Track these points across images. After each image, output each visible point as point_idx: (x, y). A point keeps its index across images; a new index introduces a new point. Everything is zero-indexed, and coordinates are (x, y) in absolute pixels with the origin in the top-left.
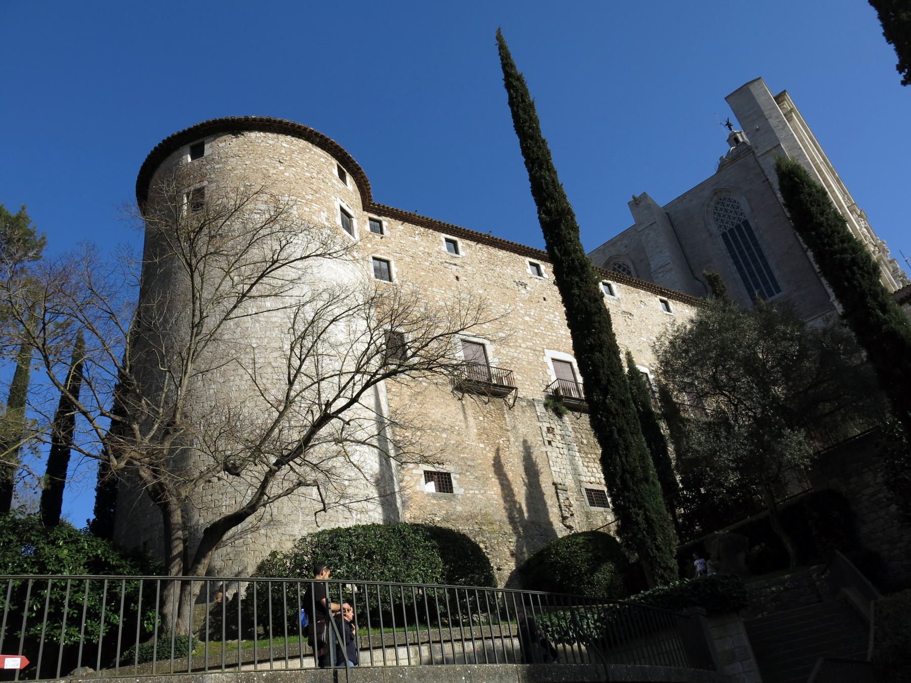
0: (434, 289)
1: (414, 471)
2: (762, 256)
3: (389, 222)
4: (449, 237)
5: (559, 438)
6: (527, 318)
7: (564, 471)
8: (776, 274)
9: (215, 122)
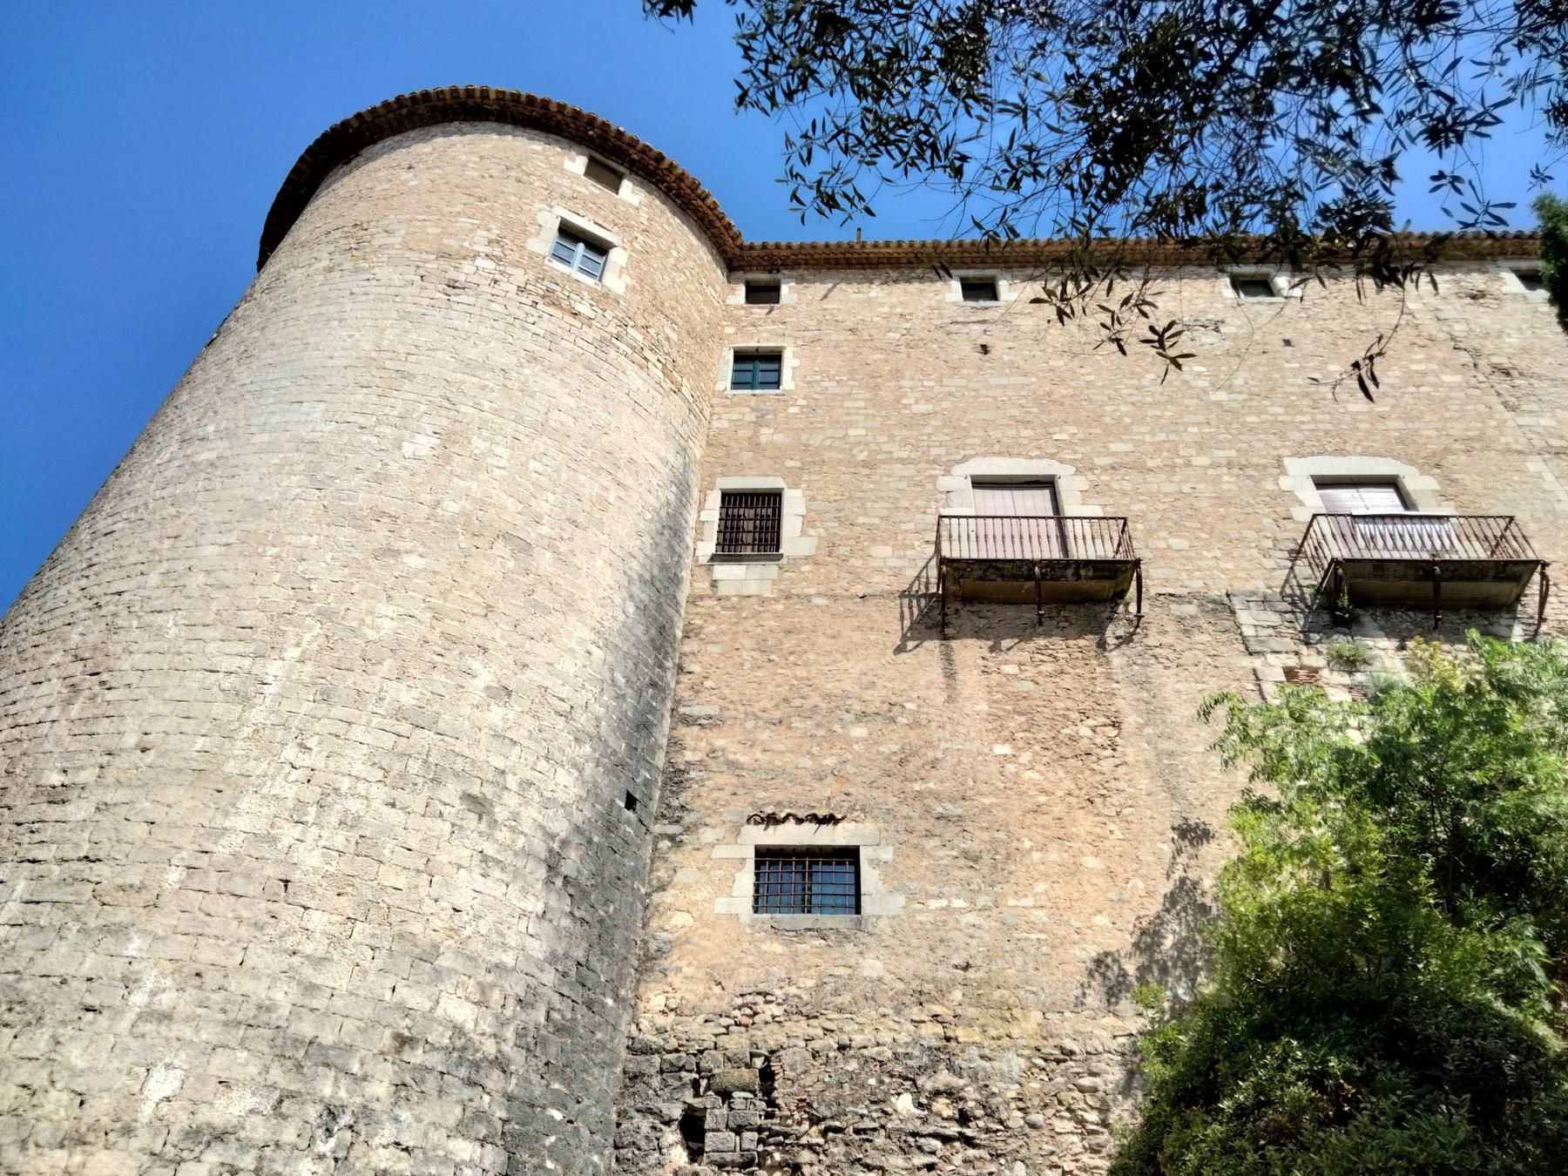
1: (720, 852)
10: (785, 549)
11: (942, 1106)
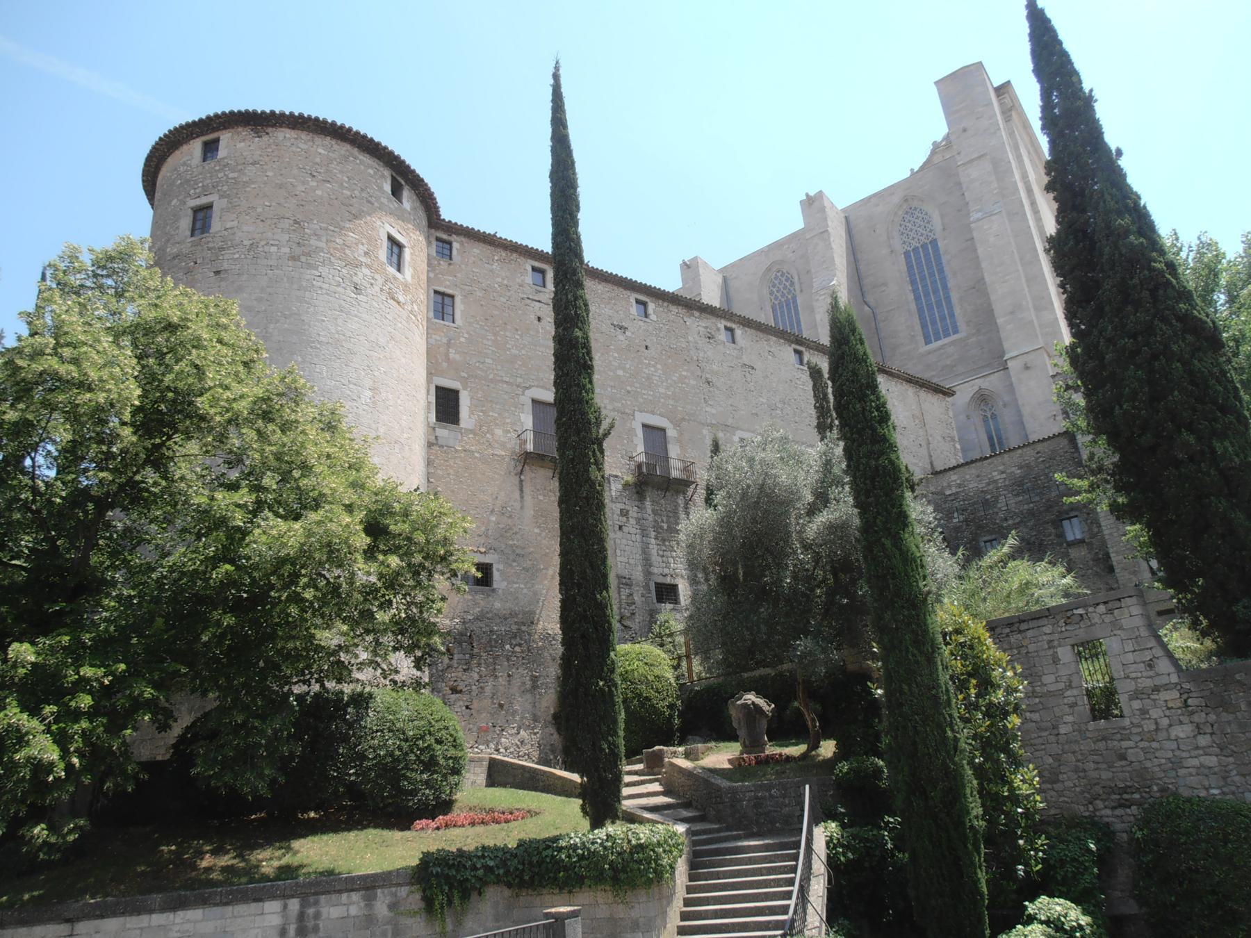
0: (508, 334)
2: (945, 287)
3: (462, 244)
4: (537, 264)
5: (632, 521)
6: (620, 373)
7: (632, 561)
8: (957, 311)
9: (232, 113)
10: (463, 424)
11: (517, 649)
